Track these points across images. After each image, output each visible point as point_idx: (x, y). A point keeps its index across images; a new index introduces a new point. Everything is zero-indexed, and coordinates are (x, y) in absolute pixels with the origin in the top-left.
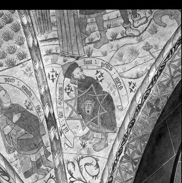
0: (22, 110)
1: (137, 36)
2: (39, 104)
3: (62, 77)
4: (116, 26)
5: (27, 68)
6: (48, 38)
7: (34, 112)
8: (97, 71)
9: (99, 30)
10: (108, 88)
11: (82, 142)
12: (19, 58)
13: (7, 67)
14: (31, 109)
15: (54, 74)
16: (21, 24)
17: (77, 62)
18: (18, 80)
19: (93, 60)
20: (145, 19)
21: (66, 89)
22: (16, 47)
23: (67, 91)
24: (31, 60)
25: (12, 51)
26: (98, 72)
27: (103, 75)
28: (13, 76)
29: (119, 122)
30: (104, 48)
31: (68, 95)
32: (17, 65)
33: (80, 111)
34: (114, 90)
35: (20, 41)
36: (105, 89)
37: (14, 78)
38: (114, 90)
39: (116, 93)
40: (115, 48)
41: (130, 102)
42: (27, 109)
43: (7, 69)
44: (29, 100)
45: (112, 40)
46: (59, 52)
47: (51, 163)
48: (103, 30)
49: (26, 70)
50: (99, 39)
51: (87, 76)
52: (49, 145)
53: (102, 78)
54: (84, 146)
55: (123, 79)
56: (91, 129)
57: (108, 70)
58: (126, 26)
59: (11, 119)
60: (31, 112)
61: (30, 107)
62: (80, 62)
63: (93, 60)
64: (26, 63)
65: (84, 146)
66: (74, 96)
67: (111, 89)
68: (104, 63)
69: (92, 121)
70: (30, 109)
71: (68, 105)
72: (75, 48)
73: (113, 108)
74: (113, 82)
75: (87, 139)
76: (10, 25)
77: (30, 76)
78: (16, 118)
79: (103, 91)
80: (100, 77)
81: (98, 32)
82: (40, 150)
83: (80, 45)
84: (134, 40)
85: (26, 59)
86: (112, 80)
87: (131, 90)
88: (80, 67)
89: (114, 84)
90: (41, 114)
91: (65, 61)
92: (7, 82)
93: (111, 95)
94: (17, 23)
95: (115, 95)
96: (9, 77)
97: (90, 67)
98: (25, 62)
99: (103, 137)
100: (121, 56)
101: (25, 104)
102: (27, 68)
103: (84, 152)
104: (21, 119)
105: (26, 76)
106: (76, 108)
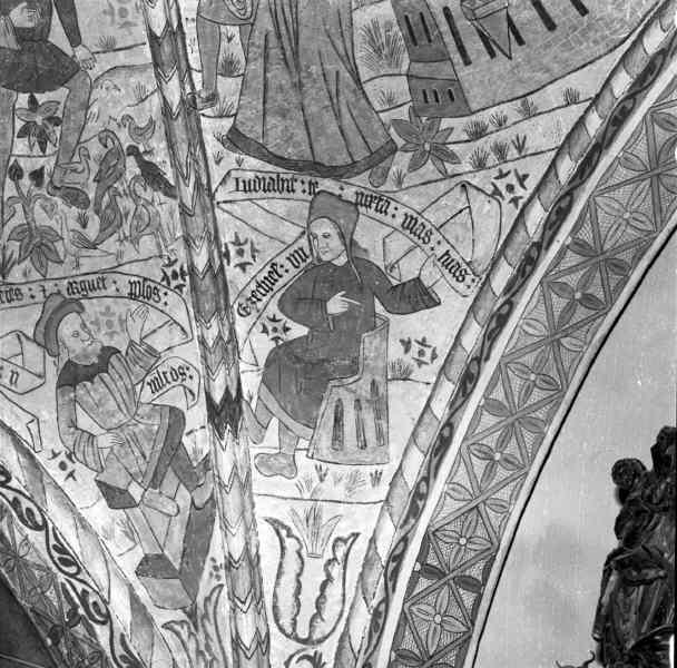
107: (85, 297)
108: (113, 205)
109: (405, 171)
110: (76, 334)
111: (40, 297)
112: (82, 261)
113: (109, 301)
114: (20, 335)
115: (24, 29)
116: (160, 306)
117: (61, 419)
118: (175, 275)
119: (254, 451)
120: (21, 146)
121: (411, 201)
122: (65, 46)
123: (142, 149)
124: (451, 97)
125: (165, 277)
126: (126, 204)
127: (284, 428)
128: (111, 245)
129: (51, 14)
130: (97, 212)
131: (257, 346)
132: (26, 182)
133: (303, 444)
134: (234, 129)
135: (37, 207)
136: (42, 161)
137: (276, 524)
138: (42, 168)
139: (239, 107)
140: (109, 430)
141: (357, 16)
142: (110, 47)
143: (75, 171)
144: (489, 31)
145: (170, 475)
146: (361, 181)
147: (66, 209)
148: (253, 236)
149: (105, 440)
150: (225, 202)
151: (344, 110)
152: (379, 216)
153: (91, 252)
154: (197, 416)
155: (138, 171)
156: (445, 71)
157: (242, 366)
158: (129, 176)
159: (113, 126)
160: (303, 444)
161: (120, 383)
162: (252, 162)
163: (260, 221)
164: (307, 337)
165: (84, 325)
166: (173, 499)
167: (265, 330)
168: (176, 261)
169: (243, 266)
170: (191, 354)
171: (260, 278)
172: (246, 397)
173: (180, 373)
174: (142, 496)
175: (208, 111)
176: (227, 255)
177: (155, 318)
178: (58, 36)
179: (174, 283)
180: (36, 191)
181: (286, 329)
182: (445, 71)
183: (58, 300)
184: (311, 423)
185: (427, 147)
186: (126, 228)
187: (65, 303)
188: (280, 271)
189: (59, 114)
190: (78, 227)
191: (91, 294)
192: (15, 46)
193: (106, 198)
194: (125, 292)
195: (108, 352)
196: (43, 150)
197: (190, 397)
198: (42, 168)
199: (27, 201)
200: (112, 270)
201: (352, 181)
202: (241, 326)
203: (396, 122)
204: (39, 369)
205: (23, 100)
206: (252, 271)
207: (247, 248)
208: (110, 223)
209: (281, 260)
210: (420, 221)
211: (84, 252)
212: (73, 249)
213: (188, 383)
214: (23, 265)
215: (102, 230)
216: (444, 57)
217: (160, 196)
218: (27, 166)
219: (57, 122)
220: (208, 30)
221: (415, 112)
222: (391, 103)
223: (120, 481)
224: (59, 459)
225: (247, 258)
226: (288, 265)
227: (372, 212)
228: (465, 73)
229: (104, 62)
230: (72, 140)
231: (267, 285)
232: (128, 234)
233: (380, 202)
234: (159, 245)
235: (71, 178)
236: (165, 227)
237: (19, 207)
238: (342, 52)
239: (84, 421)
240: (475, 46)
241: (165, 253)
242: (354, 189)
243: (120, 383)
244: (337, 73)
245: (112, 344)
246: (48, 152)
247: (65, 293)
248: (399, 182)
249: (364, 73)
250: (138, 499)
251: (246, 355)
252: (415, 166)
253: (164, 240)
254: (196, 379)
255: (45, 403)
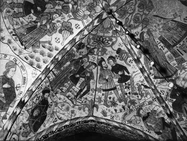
0: (13, 86)
1: (74, 105)
2: (23, 92)
3: (41, 91)
4: (73, 94)
5: (35, 73)
6: (54, 72)
7: (17, 92)
8: (52, 102)
9: (68, 89)
10: (49, 112)
11: (21, 126)
12: (37, 65)
13: (28, 63)
14: (17, 90)
15: (41, 86)
16: (53, 57)
17: (51, 91)
18: (26, 73)
19: (55, 97)
20: (81, 102)
21: (37, 97)
22: (41, 61)
23: (37, 98)
24: (41, 72)
25: (38, 60)
26: (52, 103)
27: (52, 106)
28: (26, 69)
29: (39, 131)
30: (62, 97)
31: (36, 100)
32: (33, 67)
33: (33, 111)
34: (50, 115)
35: (45, 61)
36: (47, 112)
37: (25, 70)
38: (50, 115)
39: (49, 117)
40: (64, 100)
41: (49, 126)
42: (16, 88)
43: (28, 63)
44: (20, 85)
45: (67, 97)
46: (51, 81)
47: (2, 124)
48: (68, 90)
49: (34, 73)
50: (64, 92)
51: (48, 100)
52: (10, 114)
53: (51, 106)
54: (21, 129)
55: (56, 114)
56: (29, 123)
57: (55, 106)
58: (75, 97)
59: (4, 84)
60: (16, 91)
61: (18, 89)
62: (51, 92)
63: (55, 97)
64: (37, 70)
65: (21, 129)
66: (37, 103)
67: (49, 114)
68: (57, 102)
69: (32, 120)
70: (17, 89)
71: (32, 104)
72: (55, 86)
73: (42, 123)
74: (52, 112)
75: (24, 127)
76: (49, 51)
77: (33, 77)
78: (6, 86)
79: (46, 112)
80: (51, 105)
81: (67, 89)
82: (2, 112)
83: (58, 86)
84: (72, 105)
85: (39, 69)
86: (52, 111)
87: (54, 122)
88: (49, 94)
89: (51, 113)
90: (20, 96)
91: (48, 86)
92: (21, 68)
93: (47, 116)
94: (52, 54)
95: (48, 117)
96: (24, 67)
97: (52, 98)
98: (38, 70)
99: (29, 131)
100: (63, 105)
101: (17, 85)
102: (35, 73)
103: (18, 132)
104: (7, 89)
105: (31, 75)
106: (33, 108)
107: (142, 107)
108: (142, 93)
109: (180, 73)
110: (143, 113)
111: (136, 109)
112: (140, 102)
113: (146, 106)
114: (135, 116)
115: (121, 75)
116: (154, 104)
117: (145, 125)
118: (154, 99)
119: (176, 119)
120: (126, 90)
121: (182, 76)
122: (128, 75)
123: (143, 84)
124: (183, 60)
125: (153, 100)
126: (143, 92)
127: (179, 114)
128: (143, 98)
129: (124, 71)
130: (140, 95)
131: (170, 104)
132: (128, 95)
133: (183, 115)
134: (155, 76)
135: (131, 97)
136: (129, 91)
137: (184, 128)
138: (130, 92)
139: (154, 73)
140: (153, 124)
141: (165, 55)
142: (134, 72)
143: (135, 90)
144: (184, 50)
145: (165, 127)
146: (175, 76)
147: (135, 96)
148: (163, 89)
149: (153, 126)
150: (157, 86)
151: (168, 68)
152: (179, 80)
153: (141, 100)
154: (166, 117)
155: (144, 87)
156: (180, 57)
157: (169, 108)
158: (143, 88)
159: (138, 82)
160: (183, 115)
161: (152, 117)
162: (159, 80)
163: (163, 87)
164: (176, 100)
165: (143, 111)
166: (168, 130)
167: (170, 102)
168: (154, 97)
169: (163, 94)
170: (161, 109)
171: (166, 95)
172: (172, 112)
173: (161, 112)
174: (163, 131)
175: (150, 75)
176: (160, 93)
177: (154, 106)
178: (126, 74)
179: (154, 100)
180: (130, 95)
181: (173, 100)
182: (180, 57)
183: (138, 109)
184: (182, 112)
185: (182, 68)
186: (145, 95)
187: (139, 109)
188: (169, 93)
189: (130, 84)
190: (138, 98)
191: (143, 106)
192: (120, 77)
193: (140, 92)
194: (148, 104)
195: (148, 113)
196: (129, 89)
197: (164, 115)
198: (130, 92)
199: (129, 97)
200: (145, 102)
201: (173, 77)
202: (167, 102)
203: (176, 67)
204: (139, 119)
205: (124, 84)
206: (165, 94)
207: (163, 91)
208: (142, 95)
209: (168, 91)
210: (185, 78)
211: (140, 101)
212: (138, 101)
213: (162, 113)
214: (132, 106)
215: (141, 97)
216: (180, 56)
217: (148, 89)
218: (128, 92)
219: (130, 85)
220: (147, 65)
221: (178, 64)
222: (174, 64)
223: (158, 131)
224: (147, 131)
225: (163, 93)
226: (169, 91)
227: (177, 80)
228: (183, 57)
229: (134, 74)
230: (133, 86)
231: (167, 95)
232: (145, 96)
233: (178, 78)
234: (150, 96)
235: (134, 92)
236: (150, 93)
237: (128, 98)
238: (165, 60)
239: (149, 124)
240: (183, 52)
241: (152, 96)
242: (174, 78)
243: (152, 117)
244: (166, 63)
245: (149, 112)
246: (130, 89)
247: (139, 107)
248: (180, 74)
249: (169, 62)
250: (162, 132)
251: (169, 106)
252: (181, 71)
253: (151, 95)
254: (163, 112)
255: (142, 124)
